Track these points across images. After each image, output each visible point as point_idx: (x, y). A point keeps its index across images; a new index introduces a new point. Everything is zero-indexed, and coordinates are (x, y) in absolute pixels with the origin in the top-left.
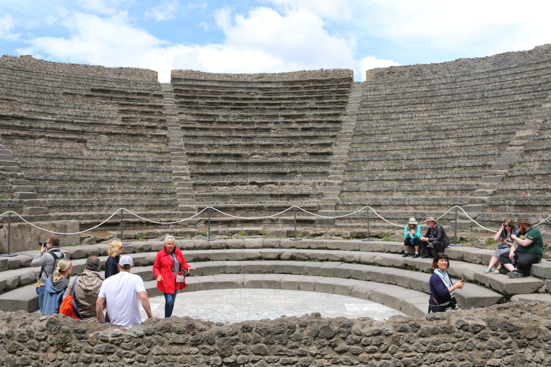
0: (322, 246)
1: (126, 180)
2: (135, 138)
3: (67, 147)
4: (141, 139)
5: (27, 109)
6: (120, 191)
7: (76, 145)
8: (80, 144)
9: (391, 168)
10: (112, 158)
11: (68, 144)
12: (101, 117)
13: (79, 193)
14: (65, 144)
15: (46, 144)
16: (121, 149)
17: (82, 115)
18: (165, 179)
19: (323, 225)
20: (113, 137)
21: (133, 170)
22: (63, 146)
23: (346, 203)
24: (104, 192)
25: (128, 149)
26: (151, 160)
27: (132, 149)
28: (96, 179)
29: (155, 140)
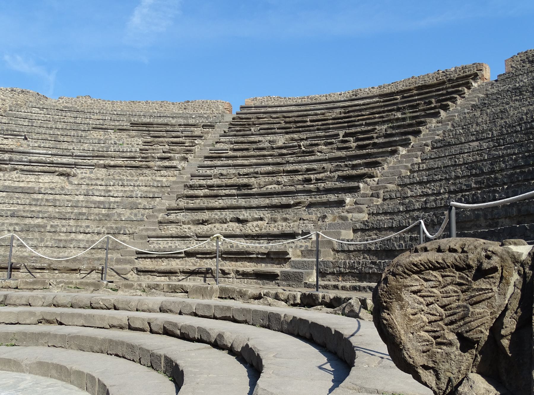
0: (228, 314)
1: (84, 217)
2: (139, 171)
3: (45, 181)
4: (147, 171)
5: (36, 145)
6: (64, 229)
7: (56, 179)
8: (62, 178)
9: (452, 188)
10: (91, 193)
11: (47, 178)
12: (123, 152)
13: (9, 231)
14: (42, 178)
15: (19, 177)
16: (112, 183)
17: (101, 150)
18: (136, 215)
19: (291, 283)
20: (112, 171)
21: (107, 206)
22: (40, 181)
23: (346, 248)
24: (43, 230)
25: (120, 183)
26: (139, 195)
27: (125, 183)
28: (46, 215)
29: (163, 172)
